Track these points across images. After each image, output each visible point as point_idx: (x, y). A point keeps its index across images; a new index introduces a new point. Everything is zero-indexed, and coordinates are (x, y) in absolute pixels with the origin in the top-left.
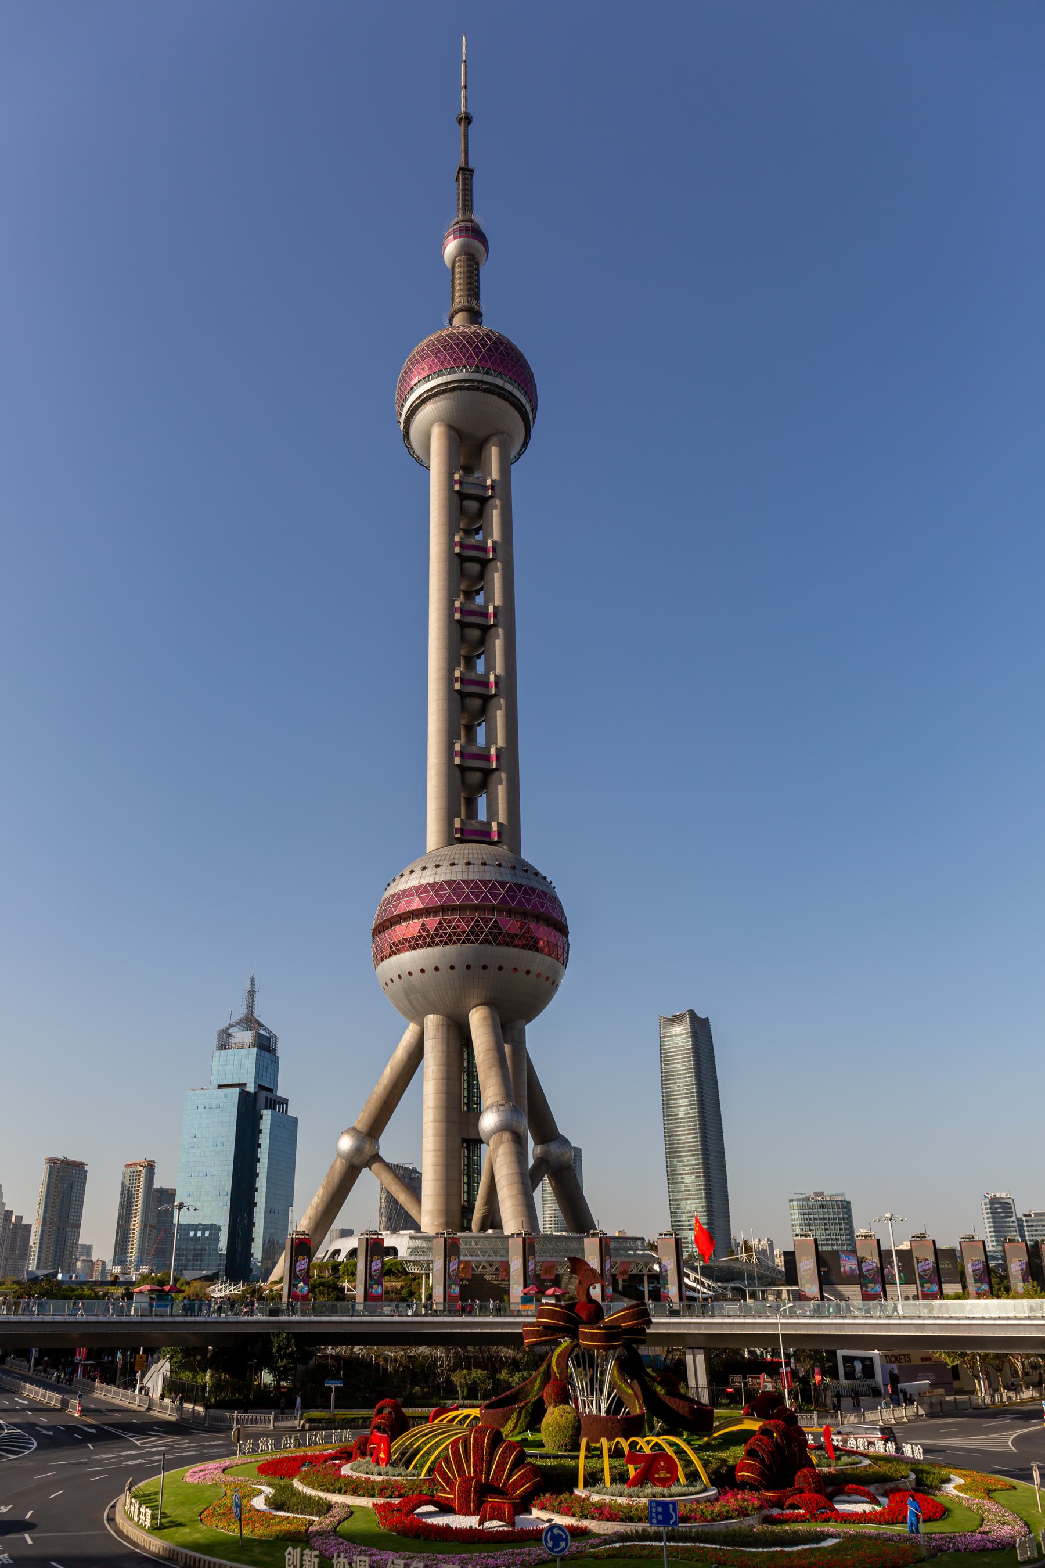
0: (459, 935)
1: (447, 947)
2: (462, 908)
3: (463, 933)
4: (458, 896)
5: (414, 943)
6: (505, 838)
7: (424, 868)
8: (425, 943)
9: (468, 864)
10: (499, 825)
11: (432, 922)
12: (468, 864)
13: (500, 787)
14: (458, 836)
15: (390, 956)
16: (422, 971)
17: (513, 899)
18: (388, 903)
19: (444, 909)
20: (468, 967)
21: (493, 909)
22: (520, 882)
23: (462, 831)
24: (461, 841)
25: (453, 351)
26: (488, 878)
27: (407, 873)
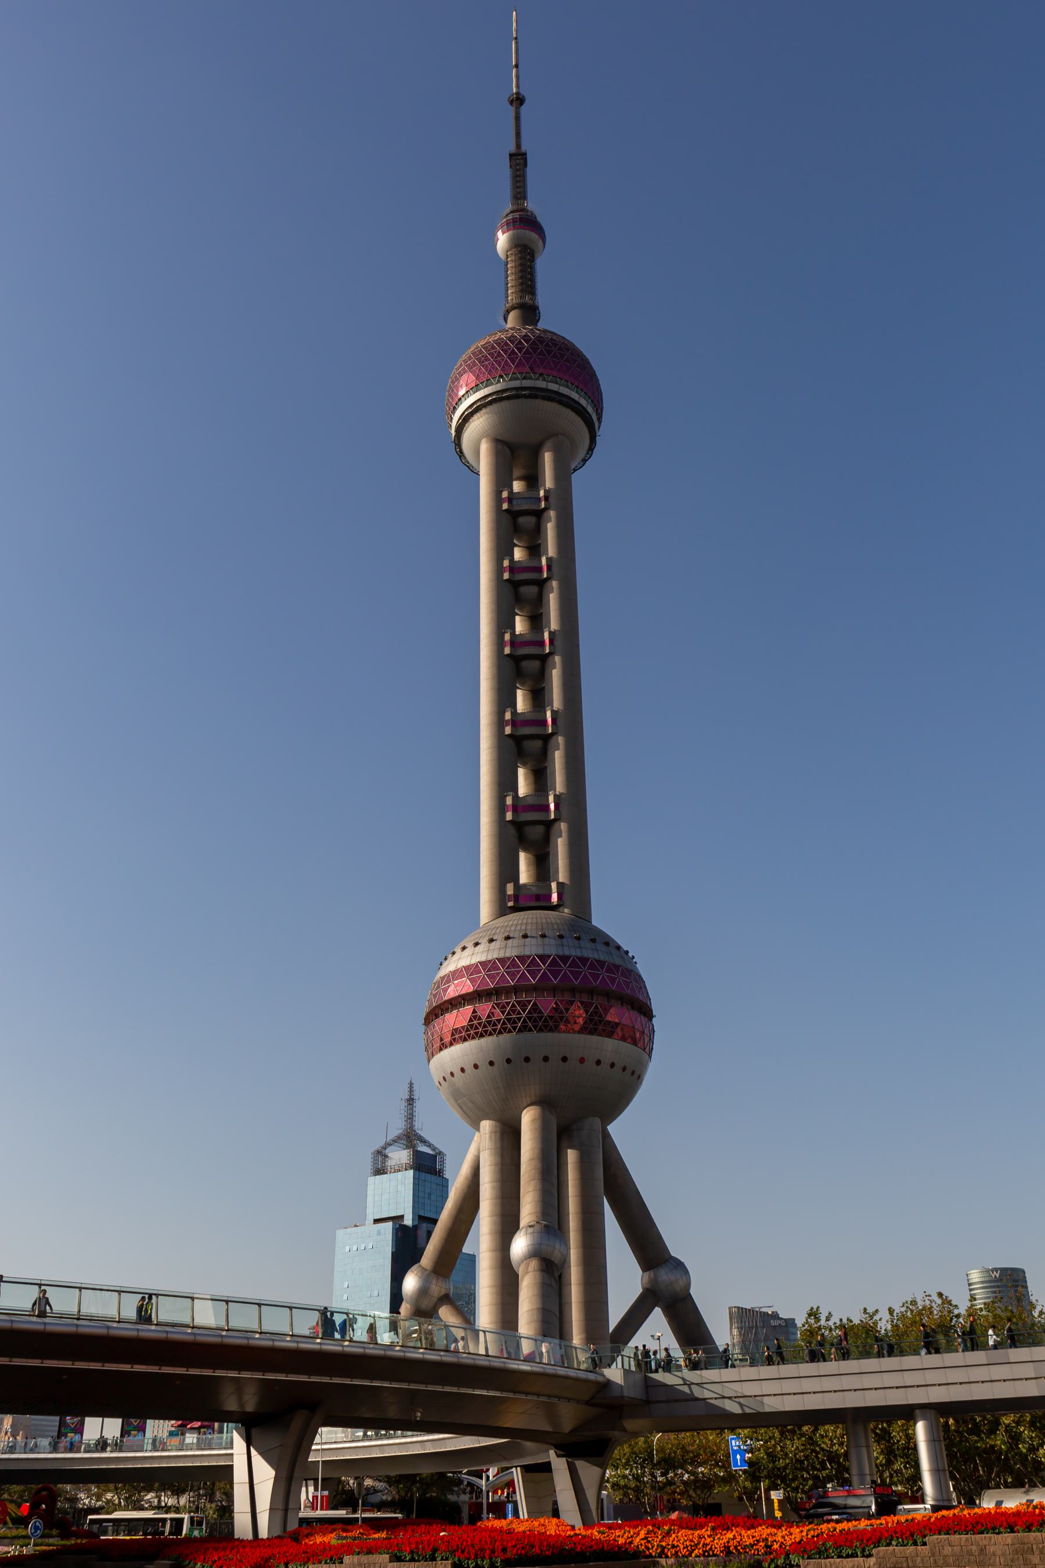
0: (515, 1022)
1: (501, 1036)
2: (516, 990)
3: (499, 1021)
4: (512, 975)
5: (459, 1036)
6: (567, 899)
7: (477, 944)
8: (476, 1033)
9: (508, 938)
10: (560, 885)
11: (485, 1008)
12: (525, 936)
13: (559, 840)
14: (510, 904)
15: (441, 1050)
16: (476, 1066)
17: (576, 975)
18: (438, 987)
19: (496, 992)
20: (508, 1061)
21: (534, 989)
22: (585, 955)
23: (516, 897)
24: (515, 909)
25: (499, 358)
26: (547, 952)
27: (458, 950)
